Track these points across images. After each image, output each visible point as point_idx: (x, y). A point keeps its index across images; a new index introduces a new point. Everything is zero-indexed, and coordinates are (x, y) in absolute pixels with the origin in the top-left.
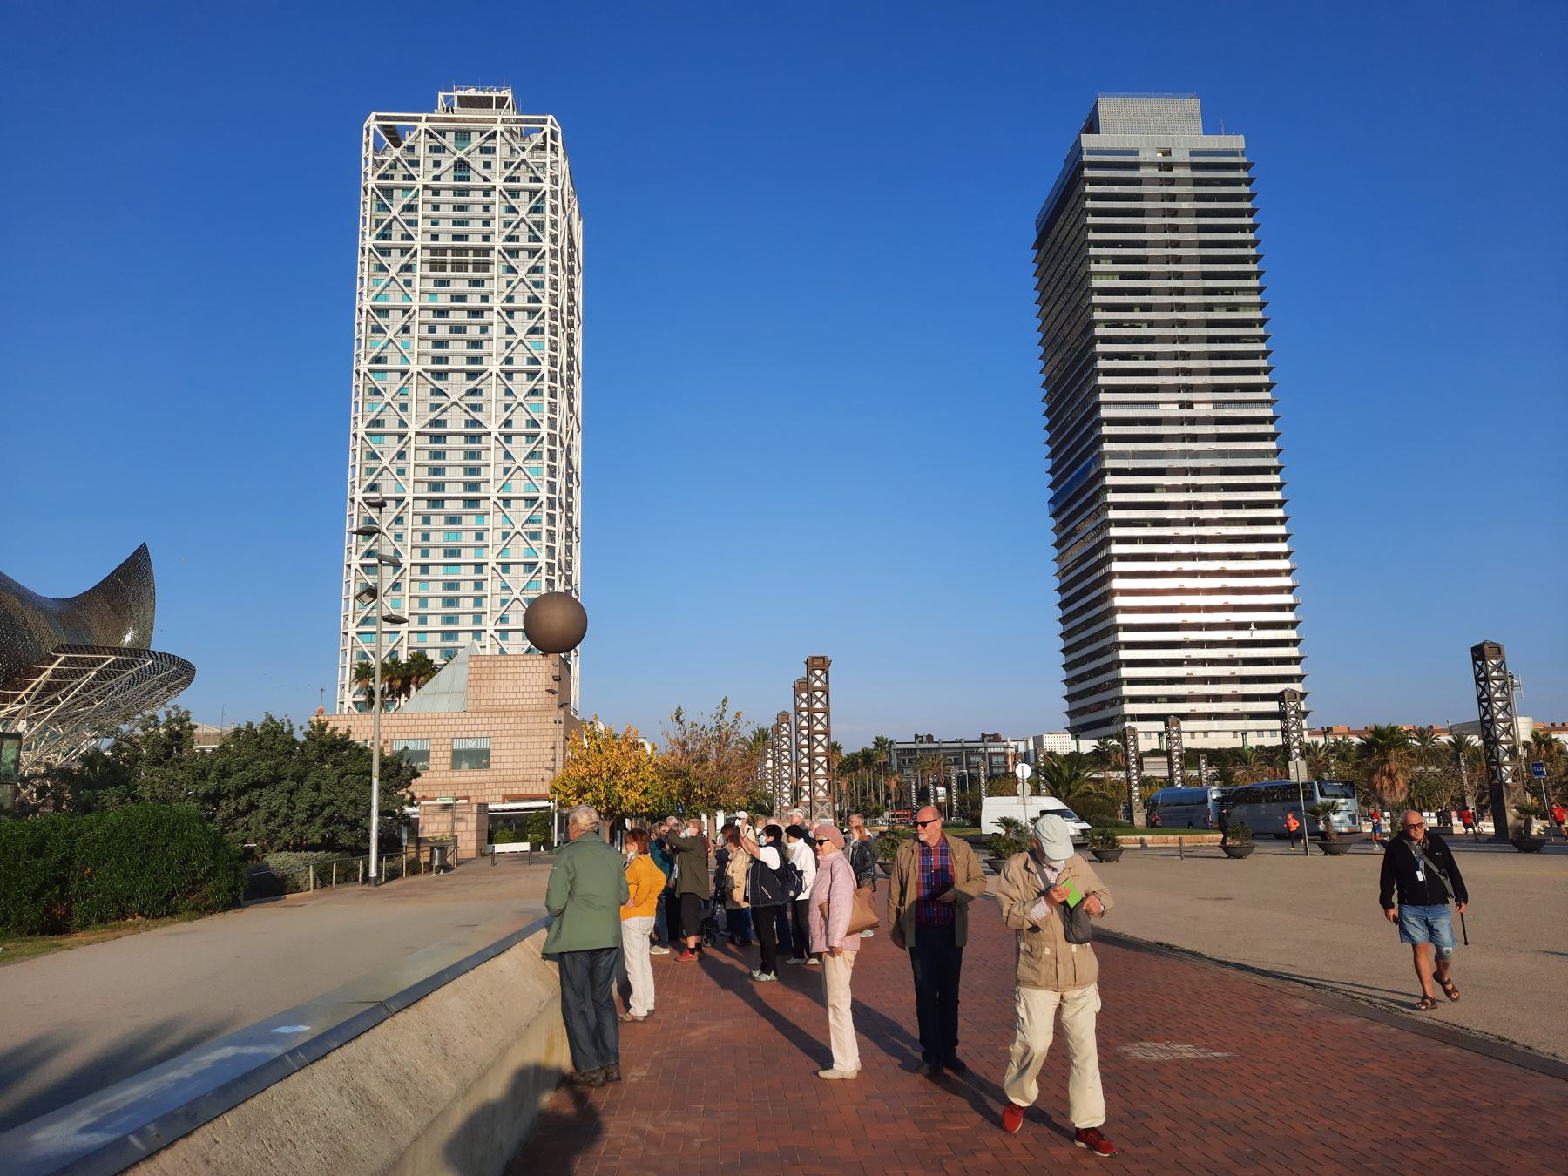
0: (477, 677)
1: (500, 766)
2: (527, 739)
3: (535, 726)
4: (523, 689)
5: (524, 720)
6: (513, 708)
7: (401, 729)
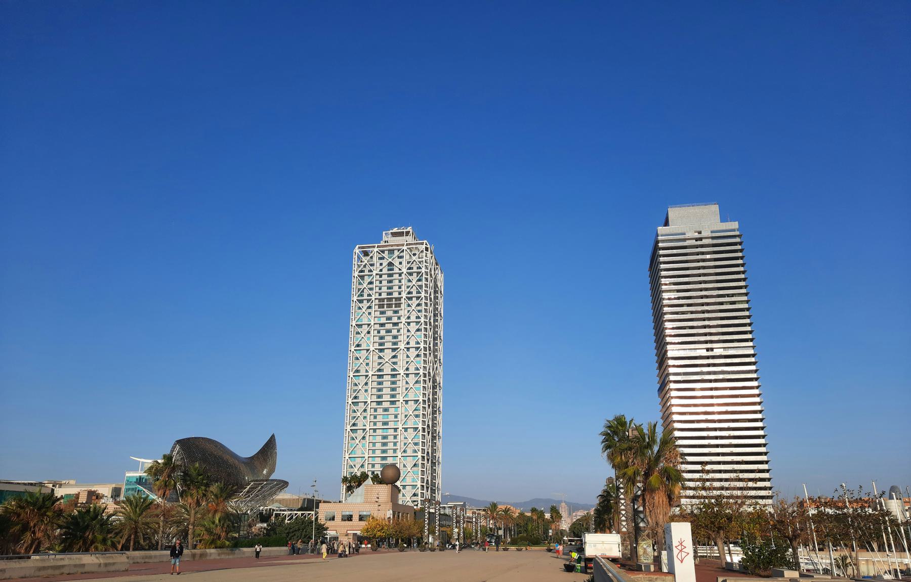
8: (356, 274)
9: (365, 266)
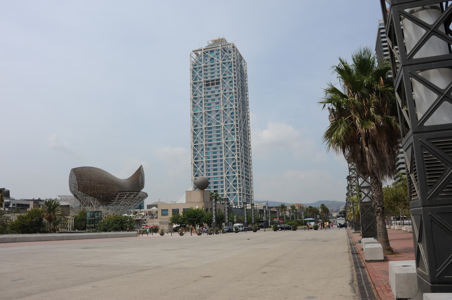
6: (194, 202)
7: (174, 207)
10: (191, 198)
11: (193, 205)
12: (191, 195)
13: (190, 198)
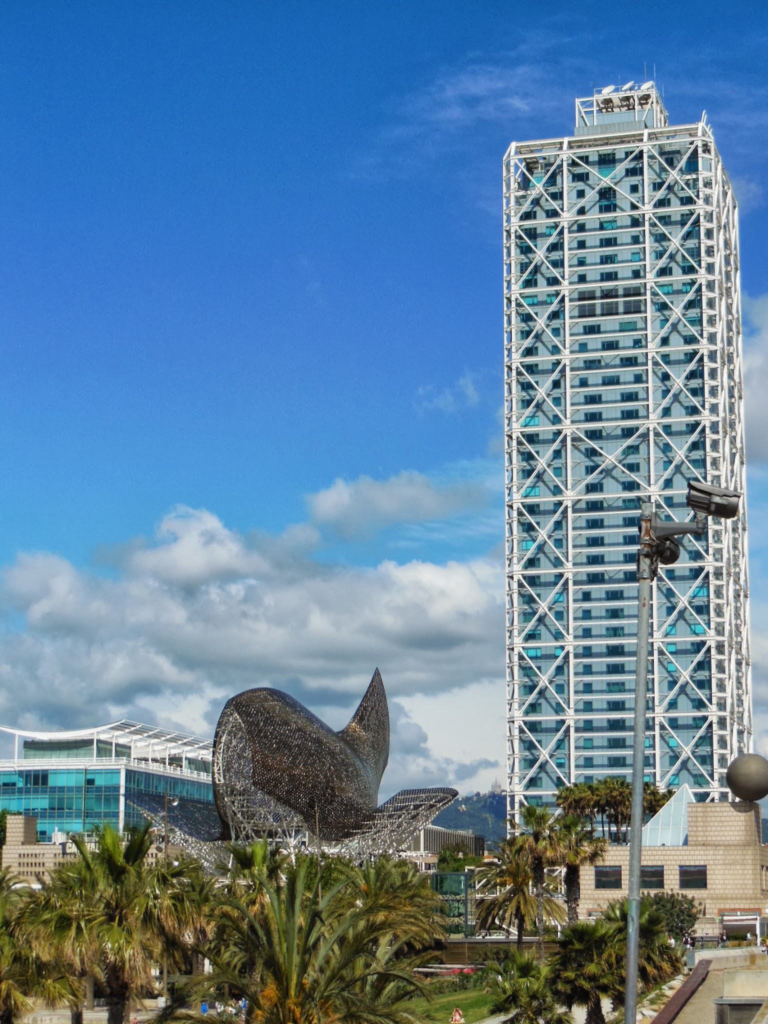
0: (694, 819)
1: (714, 886)
2: (733, 867)
3: (739, 857)
4: (728, 828)
5: (731, 852)
6: (721, 843)
8: (516, 224)
9: (536, 202)
10: (709, 829)
11: (717, 852)
12: (709, 819)
13: (705, 829)
